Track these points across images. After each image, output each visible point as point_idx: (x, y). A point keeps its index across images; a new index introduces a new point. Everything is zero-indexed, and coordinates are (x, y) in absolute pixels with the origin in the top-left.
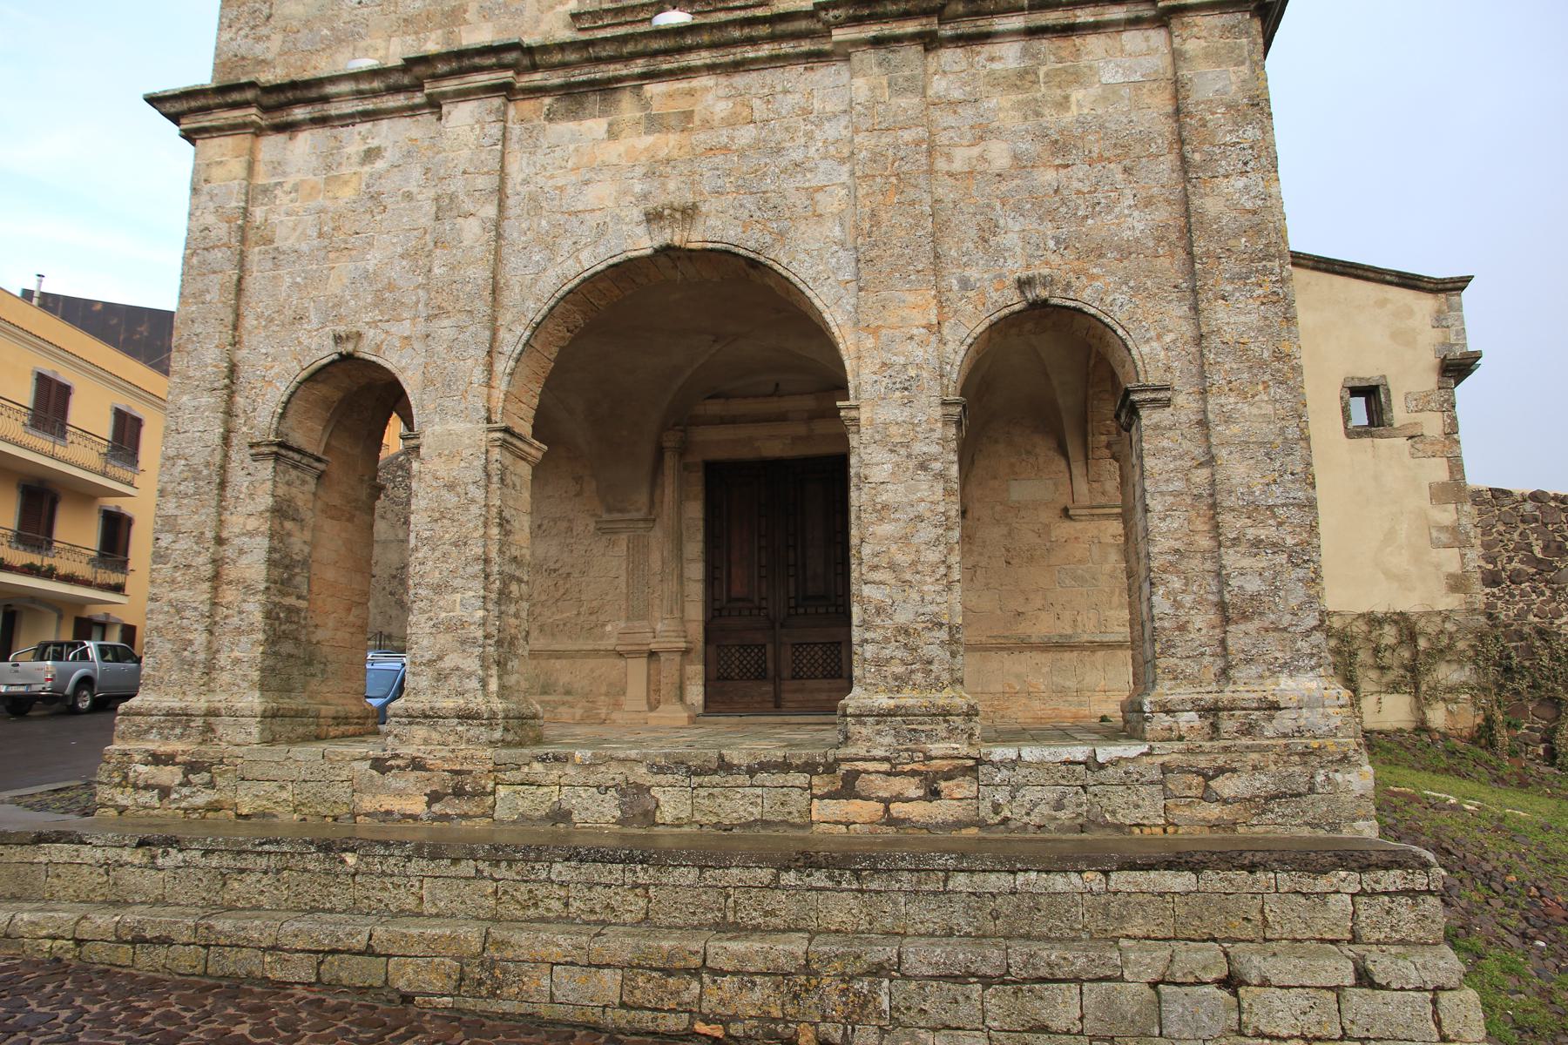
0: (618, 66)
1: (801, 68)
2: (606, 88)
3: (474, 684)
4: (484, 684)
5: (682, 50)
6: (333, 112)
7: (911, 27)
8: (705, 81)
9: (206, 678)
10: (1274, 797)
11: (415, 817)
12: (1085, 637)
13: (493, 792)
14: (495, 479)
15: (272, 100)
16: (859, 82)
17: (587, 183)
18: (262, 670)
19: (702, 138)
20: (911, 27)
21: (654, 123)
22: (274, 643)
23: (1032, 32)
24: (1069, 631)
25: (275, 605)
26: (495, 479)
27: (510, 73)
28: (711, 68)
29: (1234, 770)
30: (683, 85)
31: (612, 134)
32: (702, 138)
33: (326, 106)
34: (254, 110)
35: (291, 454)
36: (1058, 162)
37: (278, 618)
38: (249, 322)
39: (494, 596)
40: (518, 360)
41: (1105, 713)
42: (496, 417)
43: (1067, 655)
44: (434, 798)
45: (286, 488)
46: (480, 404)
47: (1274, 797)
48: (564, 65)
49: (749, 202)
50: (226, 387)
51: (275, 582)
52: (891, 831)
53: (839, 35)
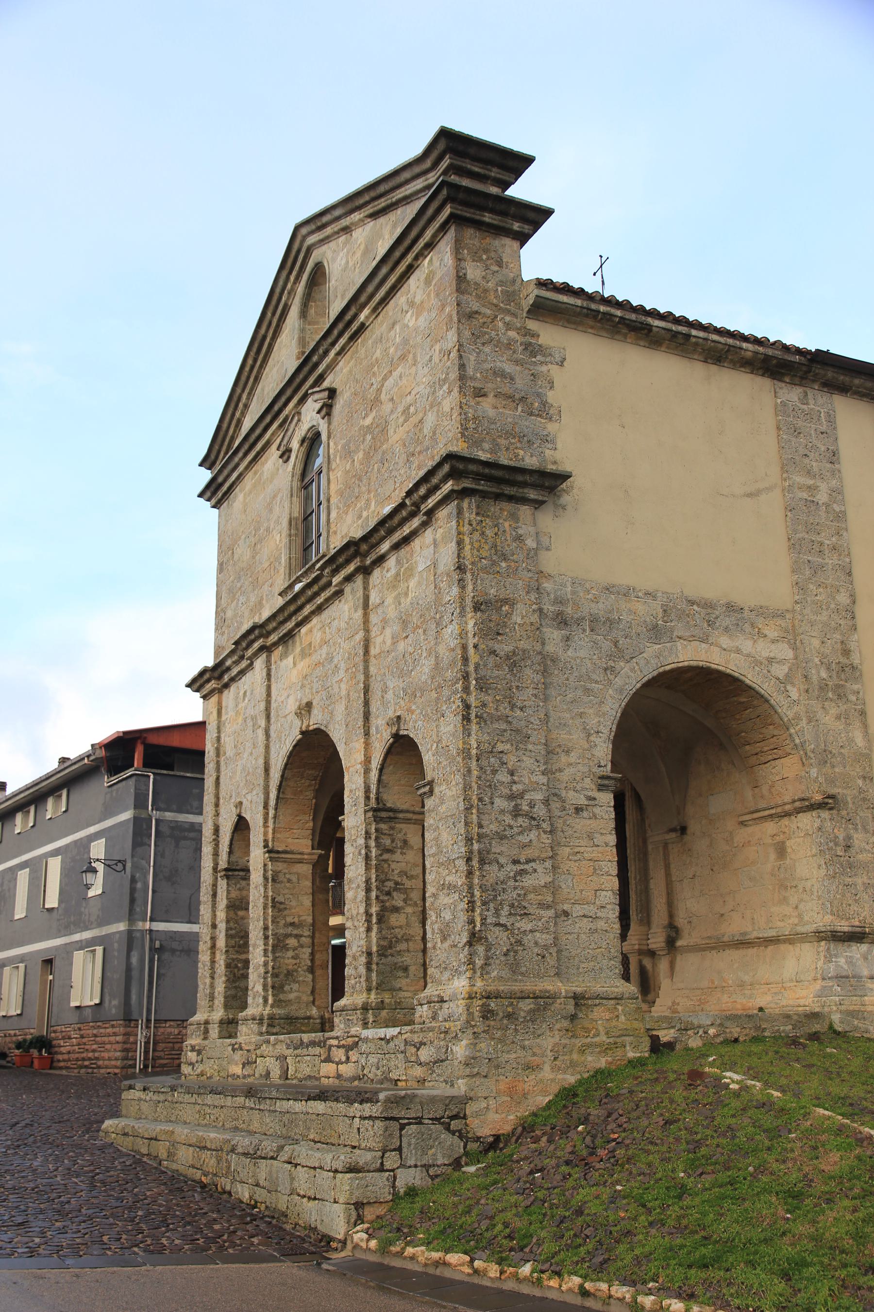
0: (289, 623)
1: (337, 601)
2: (289, 636)
3: (261, 1000)
4: (266, 1000)
5: (300, 608)
6: (233, 675)
7: (351, 568)
8: (315, 621)
9: (211, 1003)
10: (436, 1062)
11: (238, 1076)
12: (755, 934)
13: (256, 1062)
14: (270, 880)
15: (216, 674)
16: (346, 607)
17: (288, 697)
18: (225, 997)
19: (315, 658)
20: (351, 568)
21: (304, 654)
22: (234, 982)
23: (396, 547)
24: (749, 929)
25: (233, 960)
26: (270, 880)
27: (262, 640)
28: (313, 613)
29: (425, 1044)
30: (308, 626)
31: (295, 664)
32: (315, 658)
33: (230, 673)
34: (213, 682)
35: (237, 873)
36: (405, 635)
37: (236, 966)
38: (221, 801)
39: (270, 948)
40: (276, 809)
41: (762, 1004)
42: (270, 844)
43: (751, 952)
44: (244, 1065)
45: (238, 892)
46: (262, 838)
47: (436, 1062)
48: (275, 629)
49: (324, 693)
50: (214, 840)
51: (233, 947)
52: (337, 1081)
53: (336, 580)
